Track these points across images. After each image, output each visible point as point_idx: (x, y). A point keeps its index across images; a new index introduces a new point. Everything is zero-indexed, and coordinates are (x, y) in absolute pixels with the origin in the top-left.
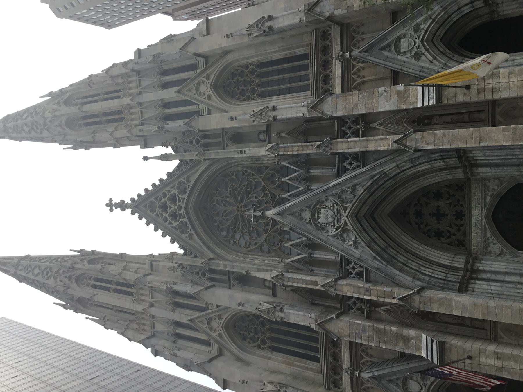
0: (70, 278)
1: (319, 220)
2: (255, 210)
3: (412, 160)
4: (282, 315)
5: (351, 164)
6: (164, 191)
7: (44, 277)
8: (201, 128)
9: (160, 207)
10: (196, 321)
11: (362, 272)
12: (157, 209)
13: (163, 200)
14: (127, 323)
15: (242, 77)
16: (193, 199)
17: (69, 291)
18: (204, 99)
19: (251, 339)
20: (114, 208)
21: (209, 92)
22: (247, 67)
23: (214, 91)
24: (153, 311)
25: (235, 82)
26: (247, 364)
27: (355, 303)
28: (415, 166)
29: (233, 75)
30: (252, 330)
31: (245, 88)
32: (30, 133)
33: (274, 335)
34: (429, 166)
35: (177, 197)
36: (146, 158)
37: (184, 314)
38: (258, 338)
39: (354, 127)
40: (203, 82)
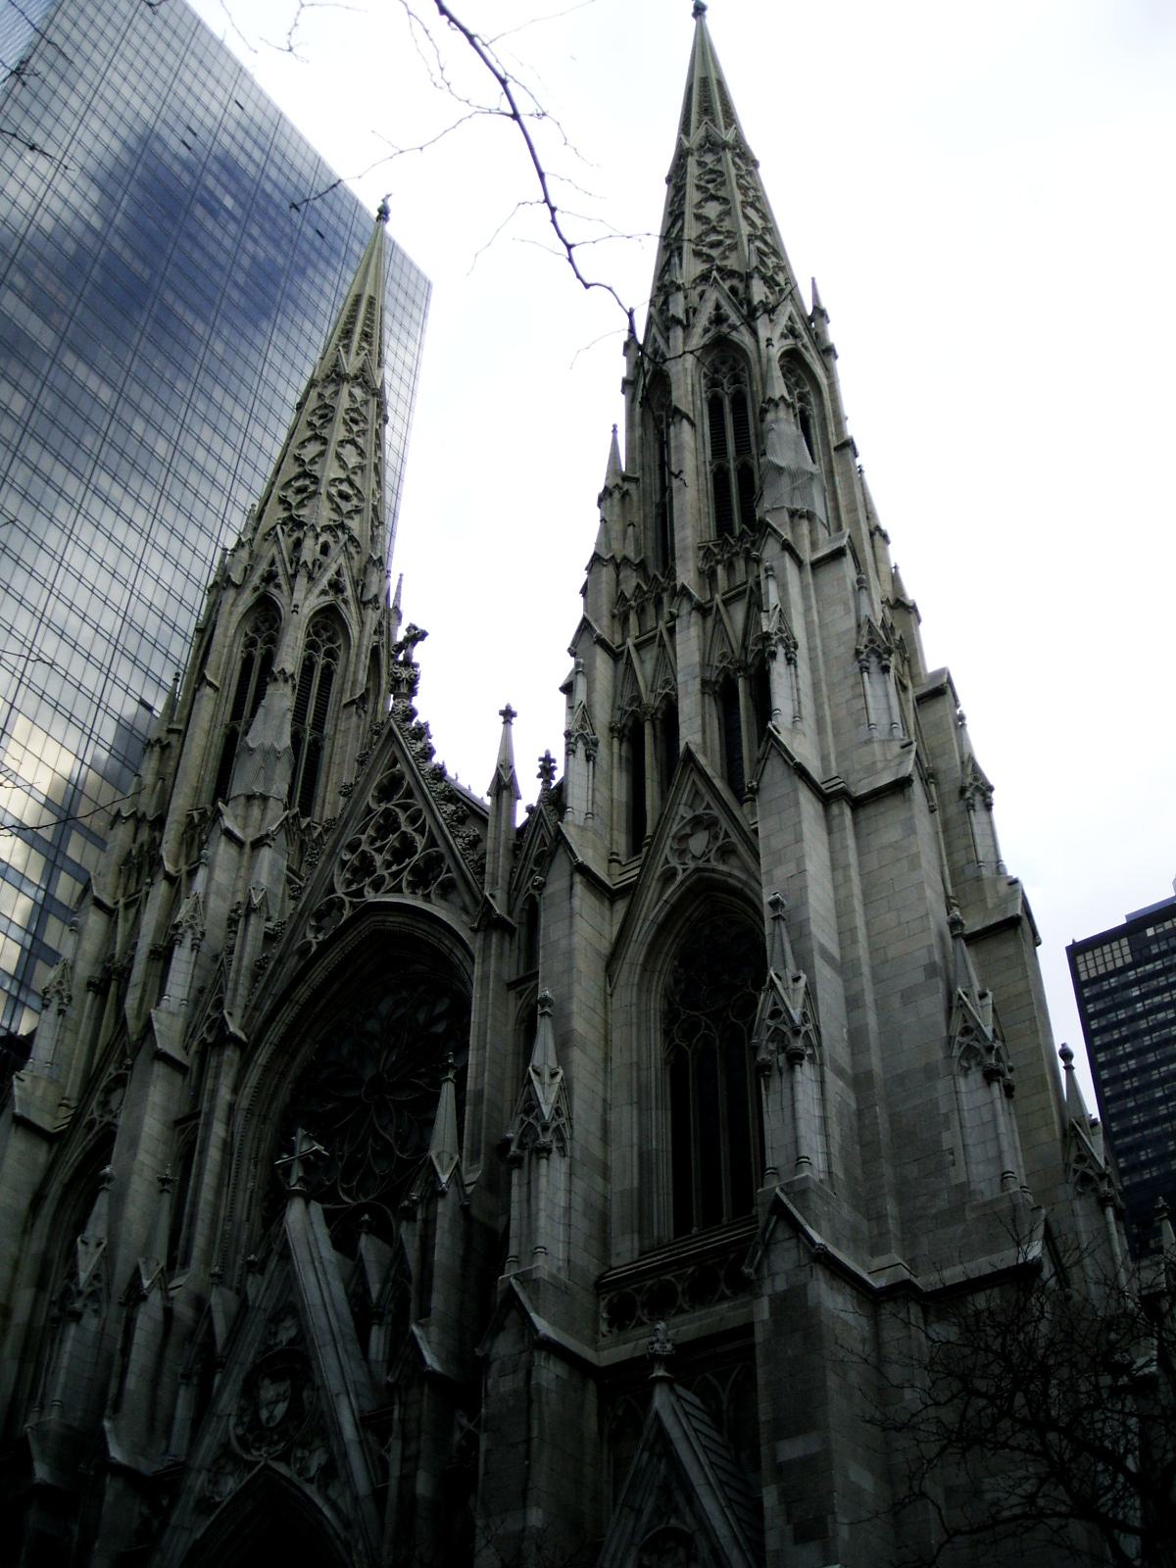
0: (270, 578)
1: (267, 1382)
2: (305, 1161)
6: (425, 814)
7: (287, 485)
9: (387, 813)
10: (126, 1038)
12: (383, 806)
13: (402, 817)
16: (394, 920)
18: (667, 861)
21: (684, 870)
23: (689, 889)
24: (161, 888)
26: (27, 1229)
36: (508, 715)
37: (144, 991)
40: (716, 838)
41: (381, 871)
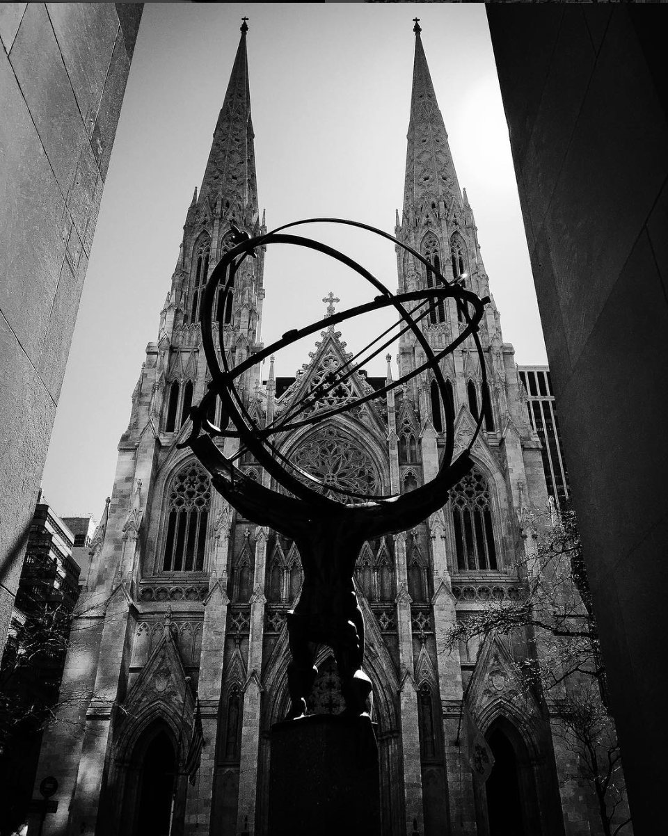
3: (388, 686)
4: (222, 539)
8: (423, 440)
11: (274, 630)
14: (182, 309)
17: (217, 222)
20: (328, 304)
22: (487, 496)
25: (471, 479)
27: (240, 621)
28: (383, 689)
30: (192, 488)
32: (419, 163)
33: (188, 516)
34: (382, 701)
35: (343, 398)
36: (389, 357)
38: (183, 496)
39: (422, 626)
41: (330, 396)
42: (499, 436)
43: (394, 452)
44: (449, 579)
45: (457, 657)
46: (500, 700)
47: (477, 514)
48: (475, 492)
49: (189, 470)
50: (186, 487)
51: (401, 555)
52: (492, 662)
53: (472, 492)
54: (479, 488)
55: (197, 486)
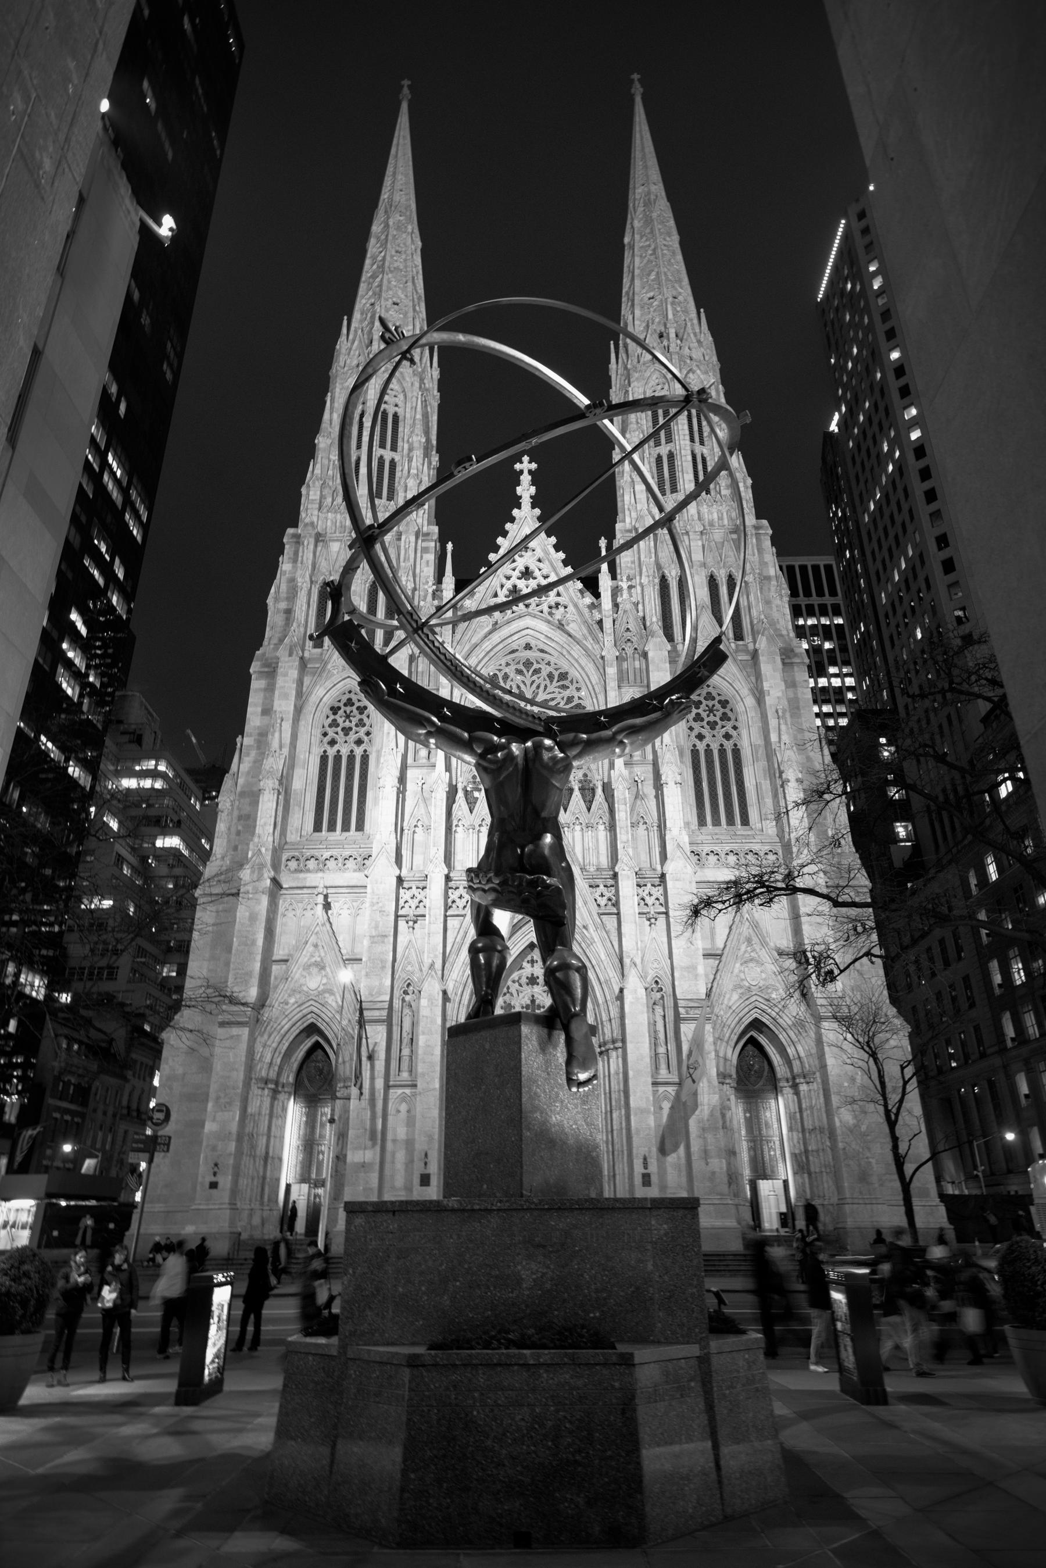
5: (602, 895)
13: (537, 573)
15: (722, 719)
19: (335, 720)
22: (735, 728)
29: (724, 703)
31: (705, 723)
38: (337, 733)
42: (751, 647)
43: (612, 671)
44: (686, 839)
45: (701, 944)
46: (754, 998)
47: (722, 751)
48: (720, 722)
49: (344, 699)
50: (340, 721)
51: (622, 807)
52: (743, 947)
53: (716, 723)
54: (725, 717)
55: (355, 721)
